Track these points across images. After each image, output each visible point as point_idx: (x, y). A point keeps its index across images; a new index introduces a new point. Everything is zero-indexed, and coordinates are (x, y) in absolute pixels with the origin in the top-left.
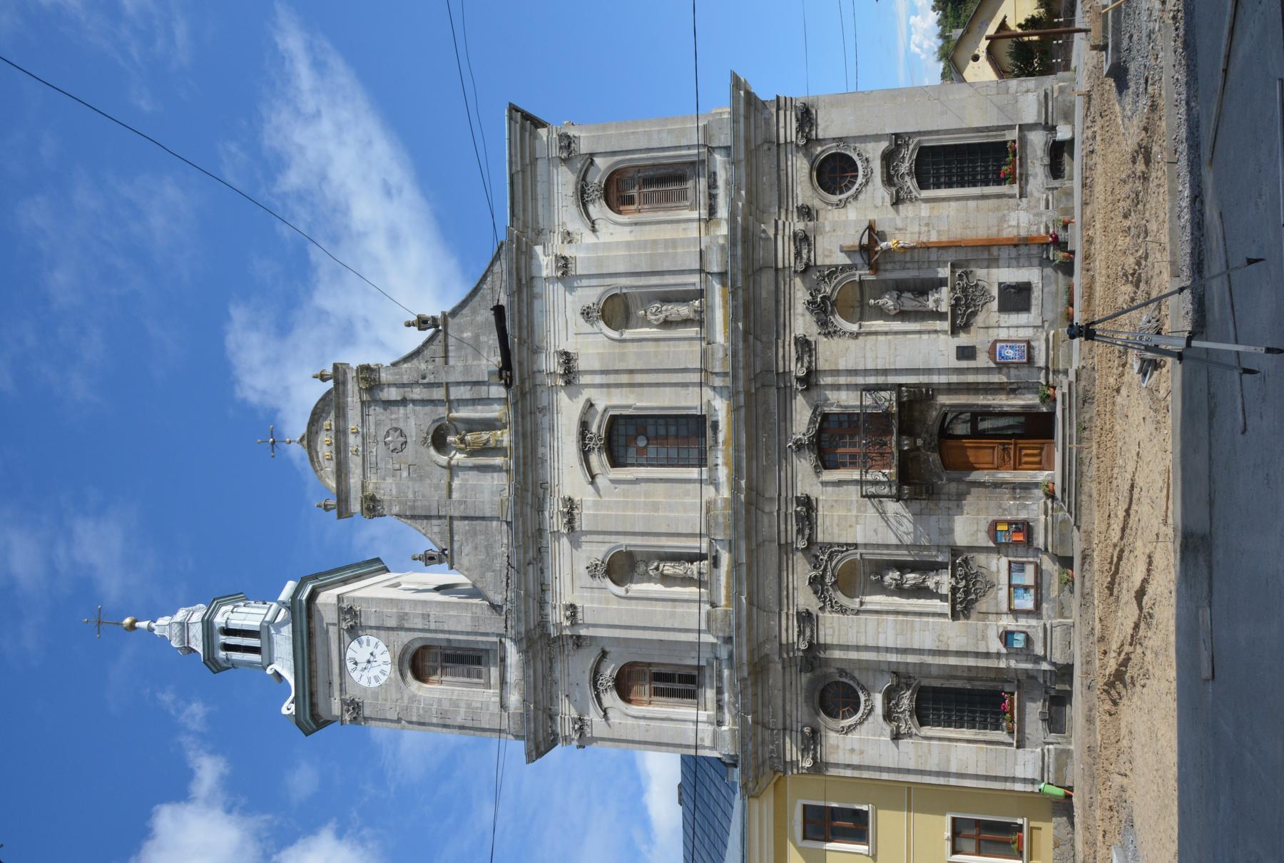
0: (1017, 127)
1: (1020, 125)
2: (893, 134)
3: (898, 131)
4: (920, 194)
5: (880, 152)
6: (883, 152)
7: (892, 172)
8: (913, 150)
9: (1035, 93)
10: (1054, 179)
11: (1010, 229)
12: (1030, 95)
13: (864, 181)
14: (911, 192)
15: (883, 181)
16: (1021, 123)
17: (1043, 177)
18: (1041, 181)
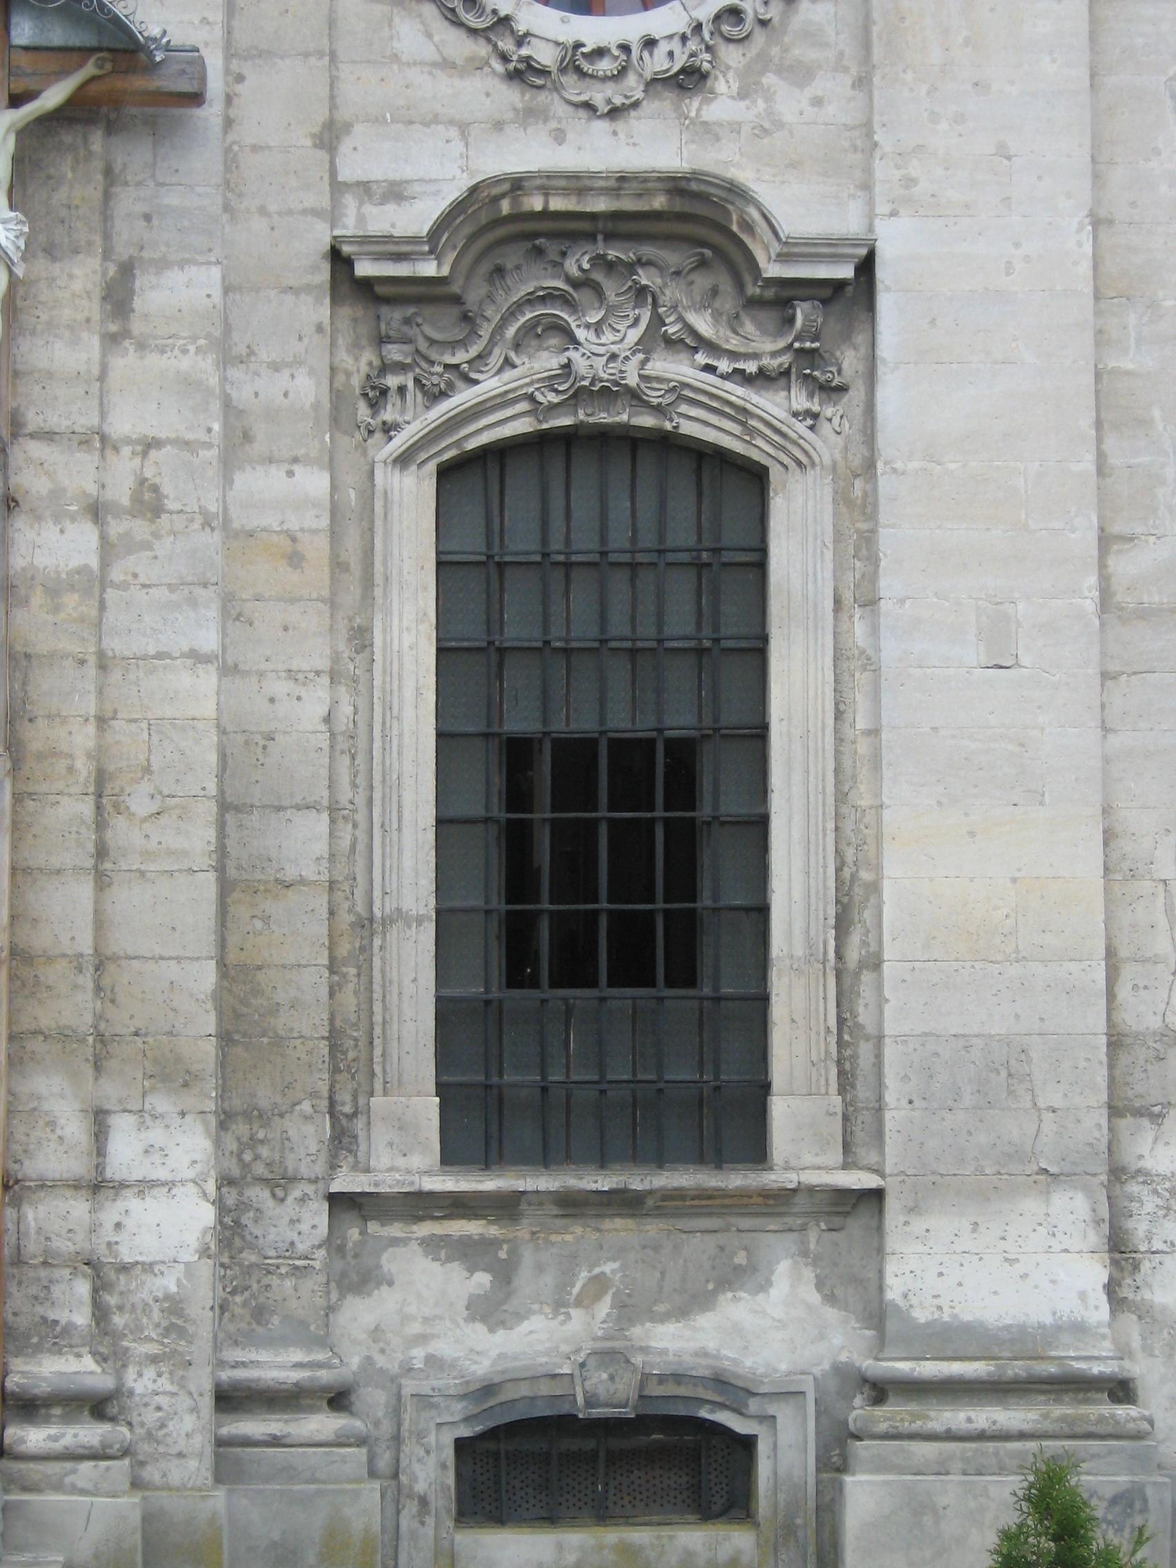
0: (869, 1181)
1: (877, 1195)
2: (866, 266)
3: (884, 301)
4: (403, 460)
5: (744, 175)
6: (736, 191)
7: (578, 262)
8: (741, 414)
9: (1099, 1311)
10: (461, 1445)
11: (75, 1128)
12: (1096, 1273)
13: (546, 56)
14: (435, 396)
15: (517, 184)
16: (892, 1205)
17: (481, 1368)
18: (443, 1348)
